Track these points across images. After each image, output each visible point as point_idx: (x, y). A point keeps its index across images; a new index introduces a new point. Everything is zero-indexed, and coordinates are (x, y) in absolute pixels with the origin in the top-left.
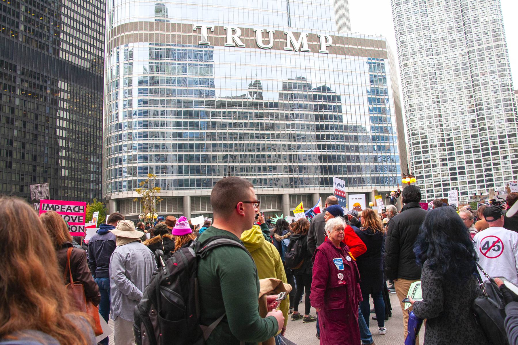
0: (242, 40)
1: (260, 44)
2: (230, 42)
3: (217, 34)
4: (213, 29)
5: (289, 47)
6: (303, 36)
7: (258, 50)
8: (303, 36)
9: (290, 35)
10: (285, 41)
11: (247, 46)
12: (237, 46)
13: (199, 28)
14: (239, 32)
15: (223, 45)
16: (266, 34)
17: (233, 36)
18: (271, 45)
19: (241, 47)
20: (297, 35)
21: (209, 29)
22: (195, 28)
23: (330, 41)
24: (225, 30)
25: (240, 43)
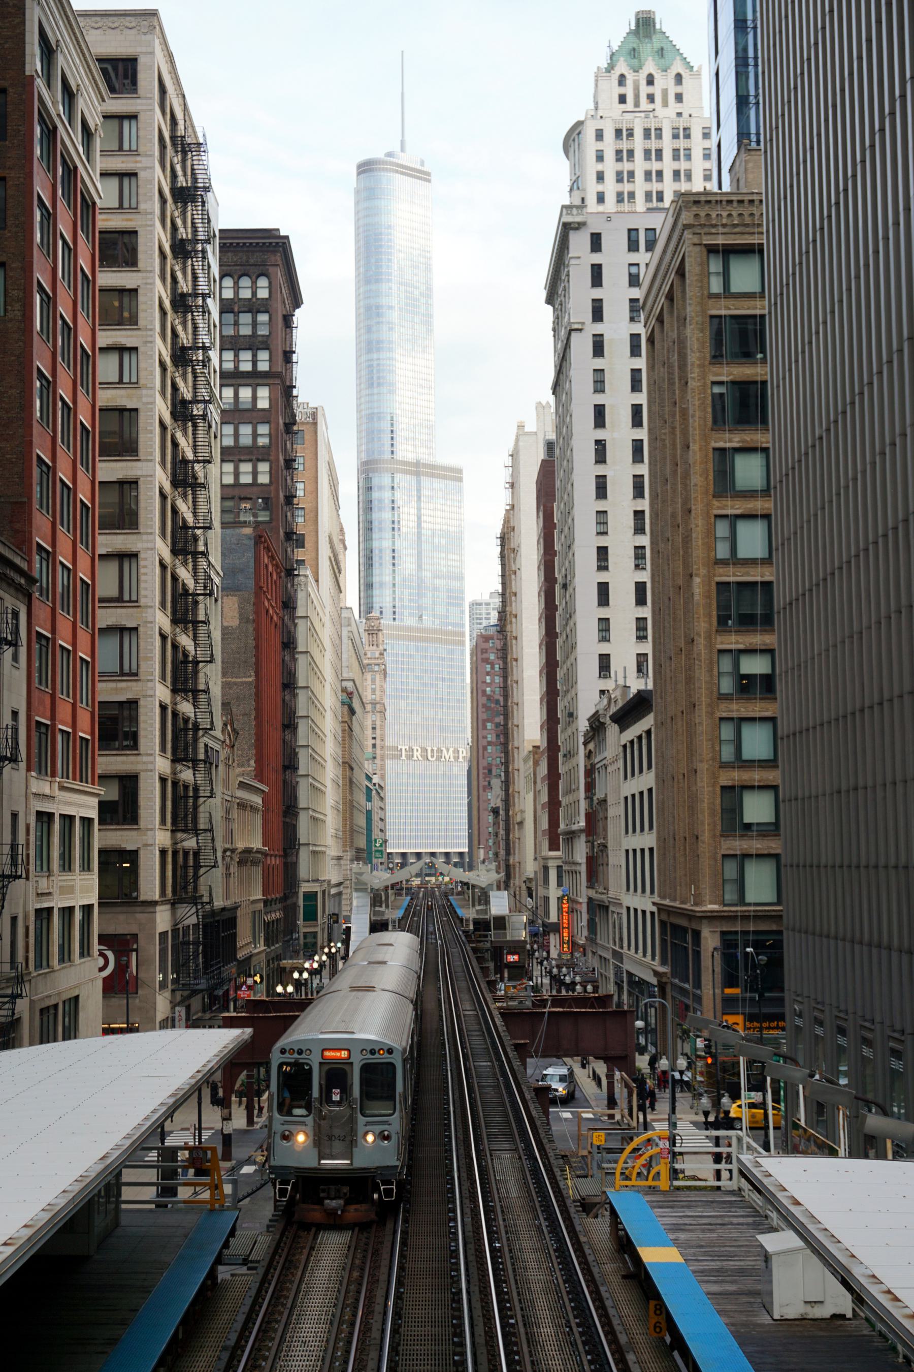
2: (415, 758)
5: (443, 759)
6: (451, 750)
8: (451, 750)
9: (444, 750)
16: (432, 750)
20: (448, 750)
23: (465, 754)
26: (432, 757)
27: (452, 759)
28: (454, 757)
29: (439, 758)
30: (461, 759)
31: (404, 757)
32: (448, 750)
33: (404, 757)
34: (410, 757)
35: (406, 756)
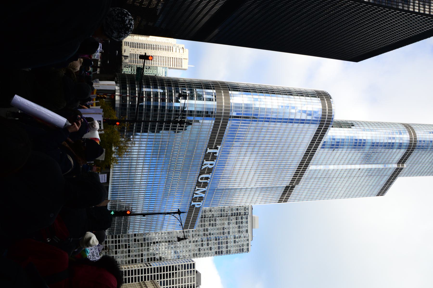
0: (206, 167)
1: (202, 176)
2: (205, 162)
3: (212, 156)
4: (215, 155)
5: (197, 188)
6: (203, 195)
7: (198, 175)
8: (203, 195)
9: (204, 189)
10: (201, 186)
11: (201, 170)
12: (202, 165)
13: (217, 148)
14: (210, 167)
15: (204, 159)
16: (207, 178)
17: (209, 164)
18: (200, 180)
19: (201, 168)
20: (204, 192)
21: (216, 153)
22: (218, 146)
23: (196, 206)
24: (213, 160)
25: (203, 167)
26: (201, 179)
27: (195, 196)
28: (196, 198)
29: (198, 184)
30: (193, 203)
31: (209, 151)
32: (204, 192)
33: (209, 151)
34: (207, 157)
35: (210, 153)
